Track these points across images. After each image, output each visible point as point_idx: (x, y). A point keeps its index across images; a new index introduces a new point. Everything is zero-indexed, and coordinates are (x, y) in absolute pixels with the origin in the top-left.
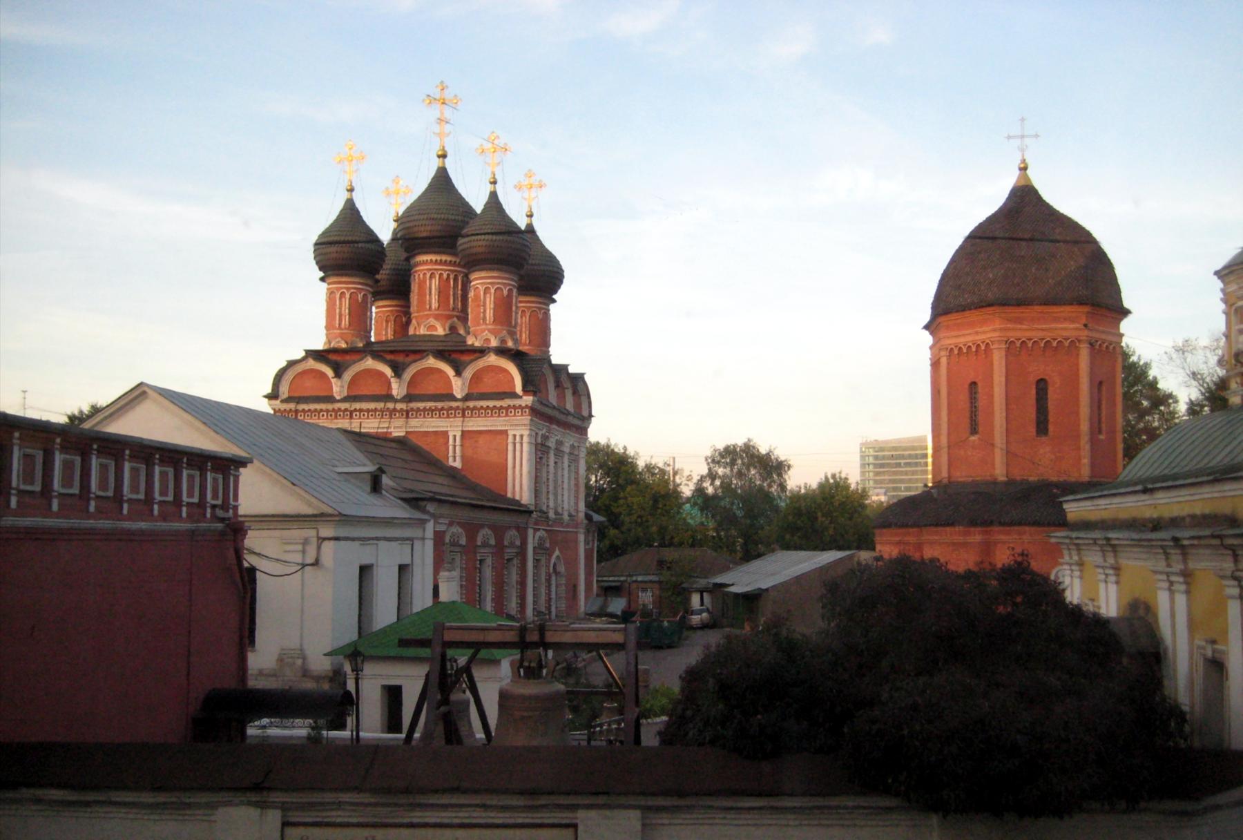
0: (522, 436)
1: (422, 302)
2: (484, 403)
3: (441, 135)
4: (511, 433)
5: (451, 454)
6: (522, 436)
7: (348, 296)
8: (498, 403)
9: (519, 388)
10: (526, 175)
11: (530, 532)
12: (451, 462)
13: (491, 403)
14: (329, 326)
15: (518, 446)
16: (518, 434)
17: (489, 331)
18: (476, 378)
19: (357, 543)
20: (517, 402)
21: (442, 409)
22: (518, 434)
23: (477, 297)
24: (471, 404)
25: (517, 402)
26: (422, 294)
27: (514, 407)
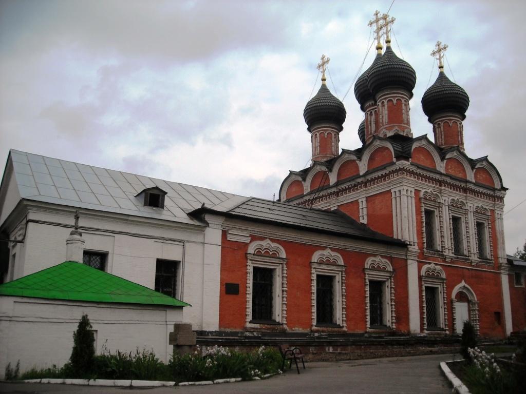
0: (400, 191)
1: (368, 131)
5: (361, 214)
8: (383, 172)
9: (394, 160)
10: (436, 46)
12: (362, 221)
13: (379, 174)
15: (398, 198)
17: (386, 129)
18: (371, 159)
20: (393, 168)
21: (355, 186)
24: (369, 177)
25: (393, 168)
27: (393, 172)
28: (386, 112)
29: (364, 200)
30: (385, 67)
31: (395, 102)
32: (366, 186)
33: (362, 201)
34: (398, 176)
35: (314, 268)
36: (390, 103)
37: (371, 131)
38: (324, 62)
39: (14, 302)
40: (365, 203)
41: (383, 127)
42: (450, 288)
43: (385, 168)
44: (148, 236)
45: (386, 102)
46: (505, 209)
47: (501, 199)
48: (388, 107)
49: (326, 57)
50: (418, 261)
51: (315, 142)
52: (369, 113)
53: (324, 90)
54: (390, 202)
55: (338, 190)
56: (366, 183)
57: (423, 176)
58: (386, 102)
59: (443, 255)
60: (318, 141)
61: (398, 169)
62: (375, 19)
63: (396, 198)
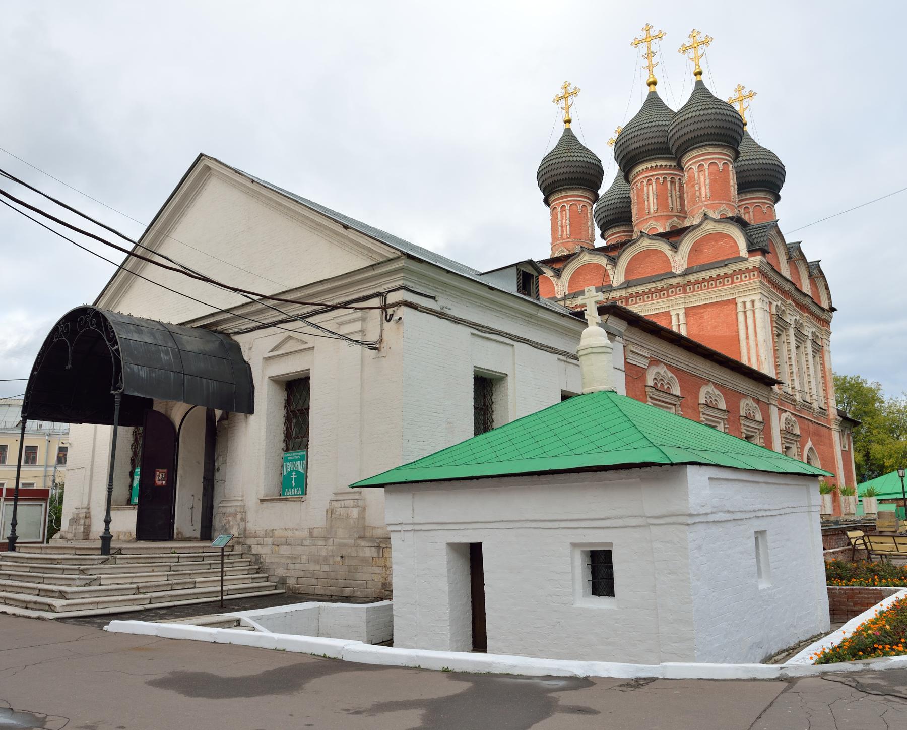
0: (753, 302)
2: (706, 275)
3: (650, 68)
4: (739, 301)
6: (753, 302)
7: (567, 208)
8: (721, 272)
9: (743, 253)
10: (735, 90)
11: (774, 411)
13: (713, 273)
14: (554, 238)
15: (749, 314)
16: (748, 300)
17: (707, 206)
18: (696, 249)
19: (466, 331)
20: (743, 266)
21: (662, 289)
22: (748, 300)
23: (691, 178)
24: (692, 278)
25: (743, 266)
26: (641, 202)
28: (708, 181)
29: (682, 312)
30: (710, 111)
31: (721, 166)
32: (685, 292)
33: (678, 315)
34: (750, 279)
35: (704, 414)
36: (713, 168)
37: (649, 208)
38: (567, 95)
39: (710, 479)
40: (682, 317)
41: (700, 204)
42: (802, 448)
43: (726, 265)
44: (551, 348)
45: (706, 167)
46: (832, 337)
47: (827, 322)
48: (710, 174)
49: (572, 86)
50: (779, 409)
51: (562, 217)
52: (645, 182)
53: (569, 138)
54: (734, 316)
55: (628, 295)
56: (685, 286)
57: (770, 281)
58: (706, 167)
59: (794, 400)
60: (568, 217)
61: (751, 267)
62: (644, 36)
63: (745, 312)
